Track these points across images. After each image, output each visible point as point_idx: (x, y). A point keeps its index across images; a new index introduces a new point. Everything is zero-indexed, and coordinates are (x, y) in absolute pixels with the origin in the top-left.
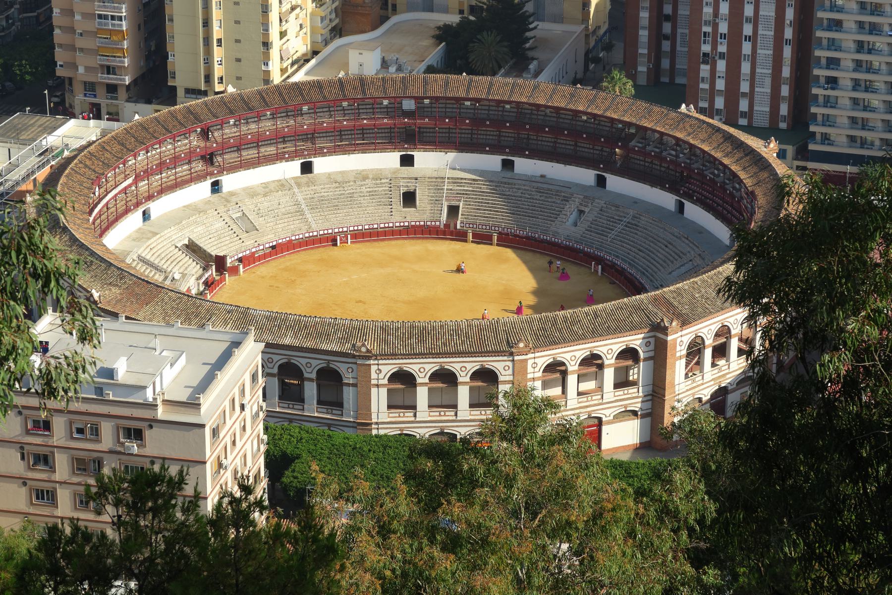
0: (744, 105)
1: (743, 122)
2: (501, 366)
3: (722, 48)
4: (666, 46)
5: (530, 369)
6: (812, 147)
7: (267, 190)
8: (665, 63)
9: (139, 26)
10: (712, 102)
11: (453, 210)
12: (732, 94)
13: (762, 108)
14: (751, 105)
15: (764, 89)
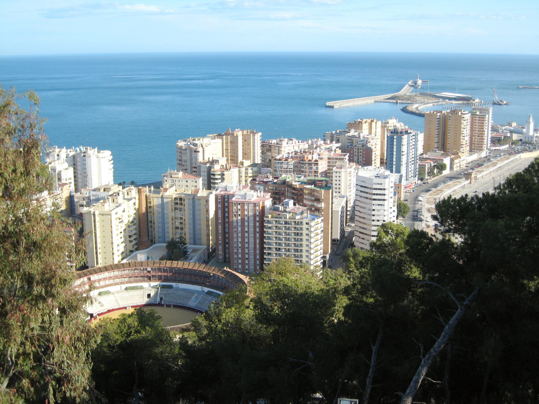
0: (247, 267)
1: (247, 272)
3: (240, 251)
4: (227, 251)
8: (227, 256)
10: (238, 267)
11: (161, 299)
12: (243, 264)
13: (252, 267)
14: (249, 267)
15: (252, 262)
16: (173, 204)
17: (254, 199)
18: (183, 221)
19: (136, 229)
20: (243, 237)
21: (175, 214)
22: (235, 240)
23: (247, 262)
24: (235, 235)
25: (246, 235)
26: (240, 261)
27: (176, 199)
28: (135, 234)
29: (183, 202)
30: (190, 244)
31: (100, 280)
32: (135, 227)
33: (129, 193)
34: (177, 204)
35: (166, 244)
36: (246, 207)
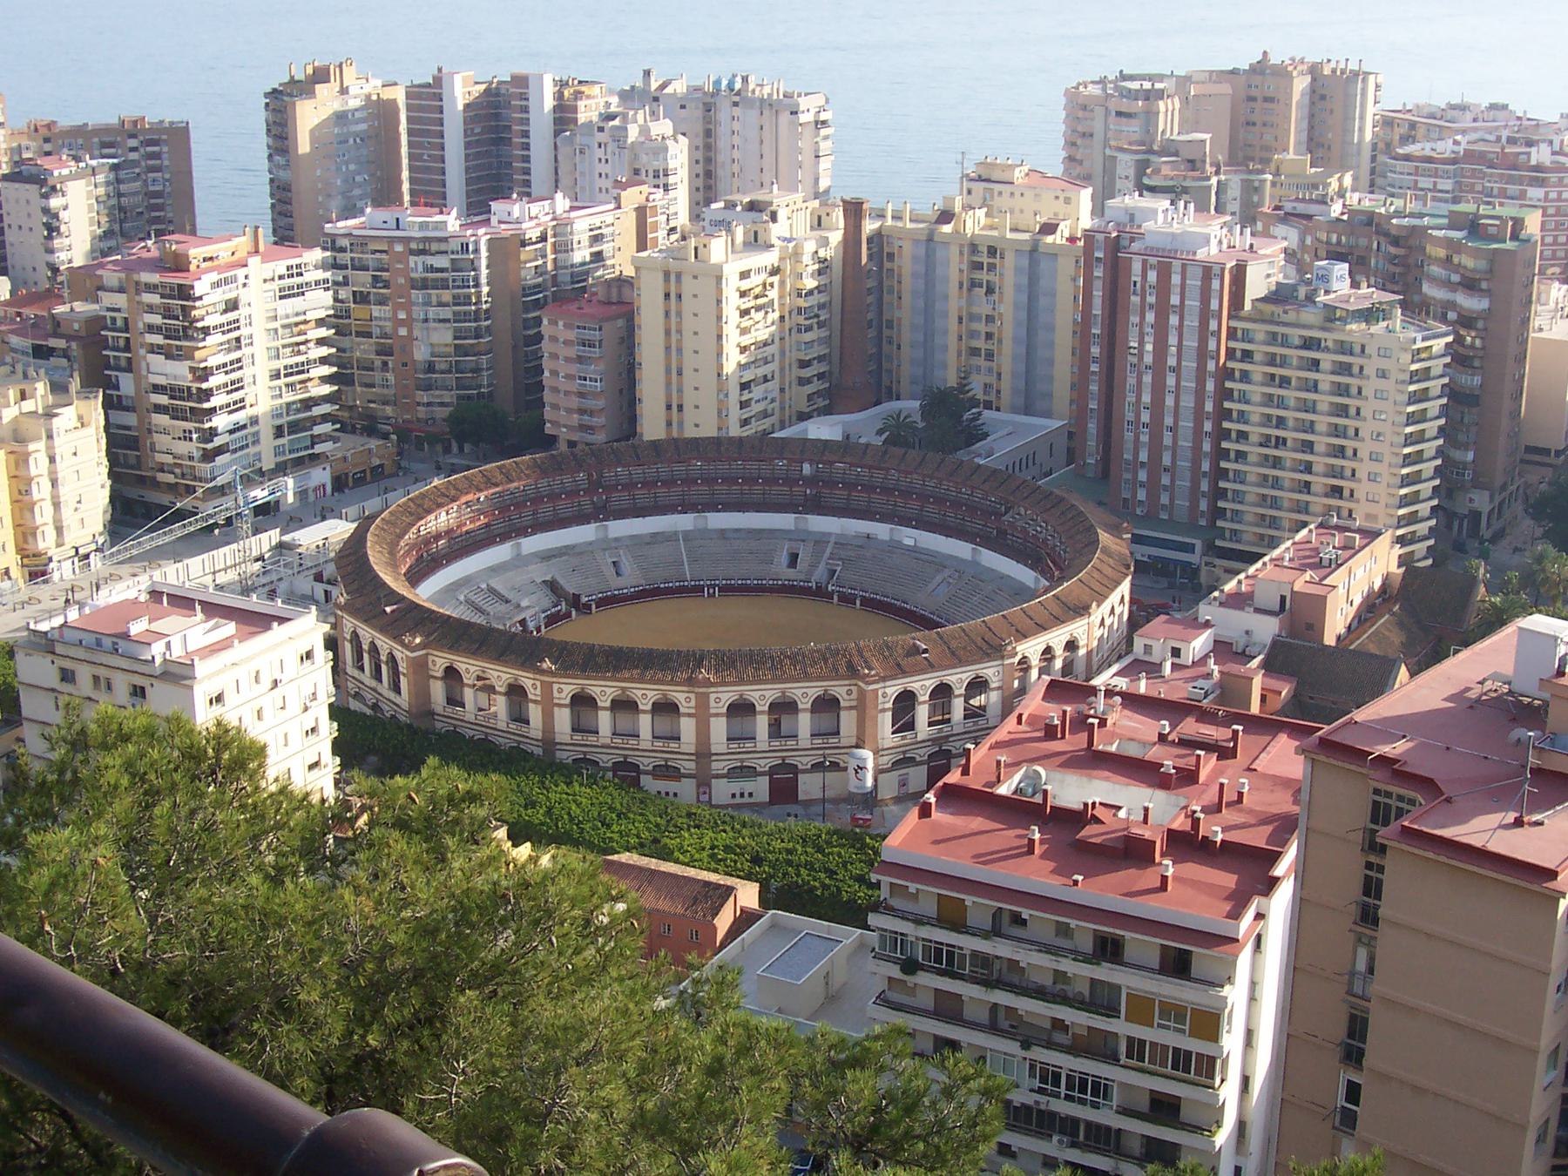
0: (1164, 499)
2: (680, 696)
5: (712, 704)
6: (1218, 543)
7: (656, 538)
9: (621, 391)
12: (1153, 486)
13: (1182, 502)
14: (1172, 500)
15: (1184, 483)
16: (965, 267)
17: (1209, 253)
18: (993, 328)
19: (827, 341)
20: (1159, 389)
21: (970, 303)
22: (1131, 398)
23: (1166, 480)
24: (1131, 380)
25: (1171, 381)
26: (1142, 476)
27: (974, 248)
28: (820, 359)
29: (997, 261)
30: (1015, 410)
31: (630, 486)
32: (824, 333)
33: (824, 218)
34: (978, 266)
35: (917, 404)
36: (1176, 279)
